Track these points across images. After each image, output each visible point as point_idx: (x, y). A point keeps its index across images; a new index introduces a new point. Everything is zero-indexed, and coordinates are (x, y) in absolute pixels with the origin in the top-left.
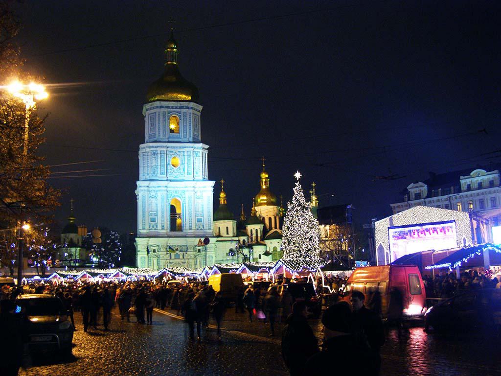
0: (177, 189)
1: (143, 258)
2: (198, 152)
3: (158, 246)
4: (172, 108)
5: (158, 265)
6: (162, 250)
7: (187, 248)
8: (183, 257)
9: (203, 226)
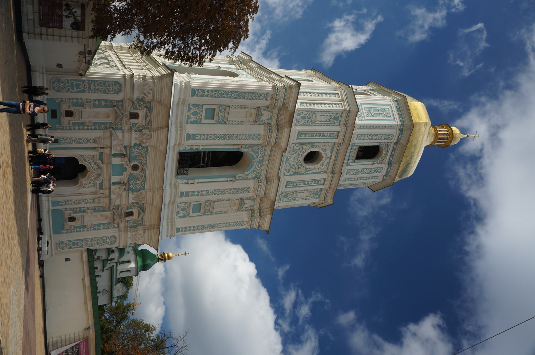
0: (266, 163)
1: (116, 88)
2: (320, 195)
3: (147, 126)
4: (394, 150)
5: (95, 124)
6: (134, 135)
7: (137, 190)
8: (114, 183)
9: (184, 216)
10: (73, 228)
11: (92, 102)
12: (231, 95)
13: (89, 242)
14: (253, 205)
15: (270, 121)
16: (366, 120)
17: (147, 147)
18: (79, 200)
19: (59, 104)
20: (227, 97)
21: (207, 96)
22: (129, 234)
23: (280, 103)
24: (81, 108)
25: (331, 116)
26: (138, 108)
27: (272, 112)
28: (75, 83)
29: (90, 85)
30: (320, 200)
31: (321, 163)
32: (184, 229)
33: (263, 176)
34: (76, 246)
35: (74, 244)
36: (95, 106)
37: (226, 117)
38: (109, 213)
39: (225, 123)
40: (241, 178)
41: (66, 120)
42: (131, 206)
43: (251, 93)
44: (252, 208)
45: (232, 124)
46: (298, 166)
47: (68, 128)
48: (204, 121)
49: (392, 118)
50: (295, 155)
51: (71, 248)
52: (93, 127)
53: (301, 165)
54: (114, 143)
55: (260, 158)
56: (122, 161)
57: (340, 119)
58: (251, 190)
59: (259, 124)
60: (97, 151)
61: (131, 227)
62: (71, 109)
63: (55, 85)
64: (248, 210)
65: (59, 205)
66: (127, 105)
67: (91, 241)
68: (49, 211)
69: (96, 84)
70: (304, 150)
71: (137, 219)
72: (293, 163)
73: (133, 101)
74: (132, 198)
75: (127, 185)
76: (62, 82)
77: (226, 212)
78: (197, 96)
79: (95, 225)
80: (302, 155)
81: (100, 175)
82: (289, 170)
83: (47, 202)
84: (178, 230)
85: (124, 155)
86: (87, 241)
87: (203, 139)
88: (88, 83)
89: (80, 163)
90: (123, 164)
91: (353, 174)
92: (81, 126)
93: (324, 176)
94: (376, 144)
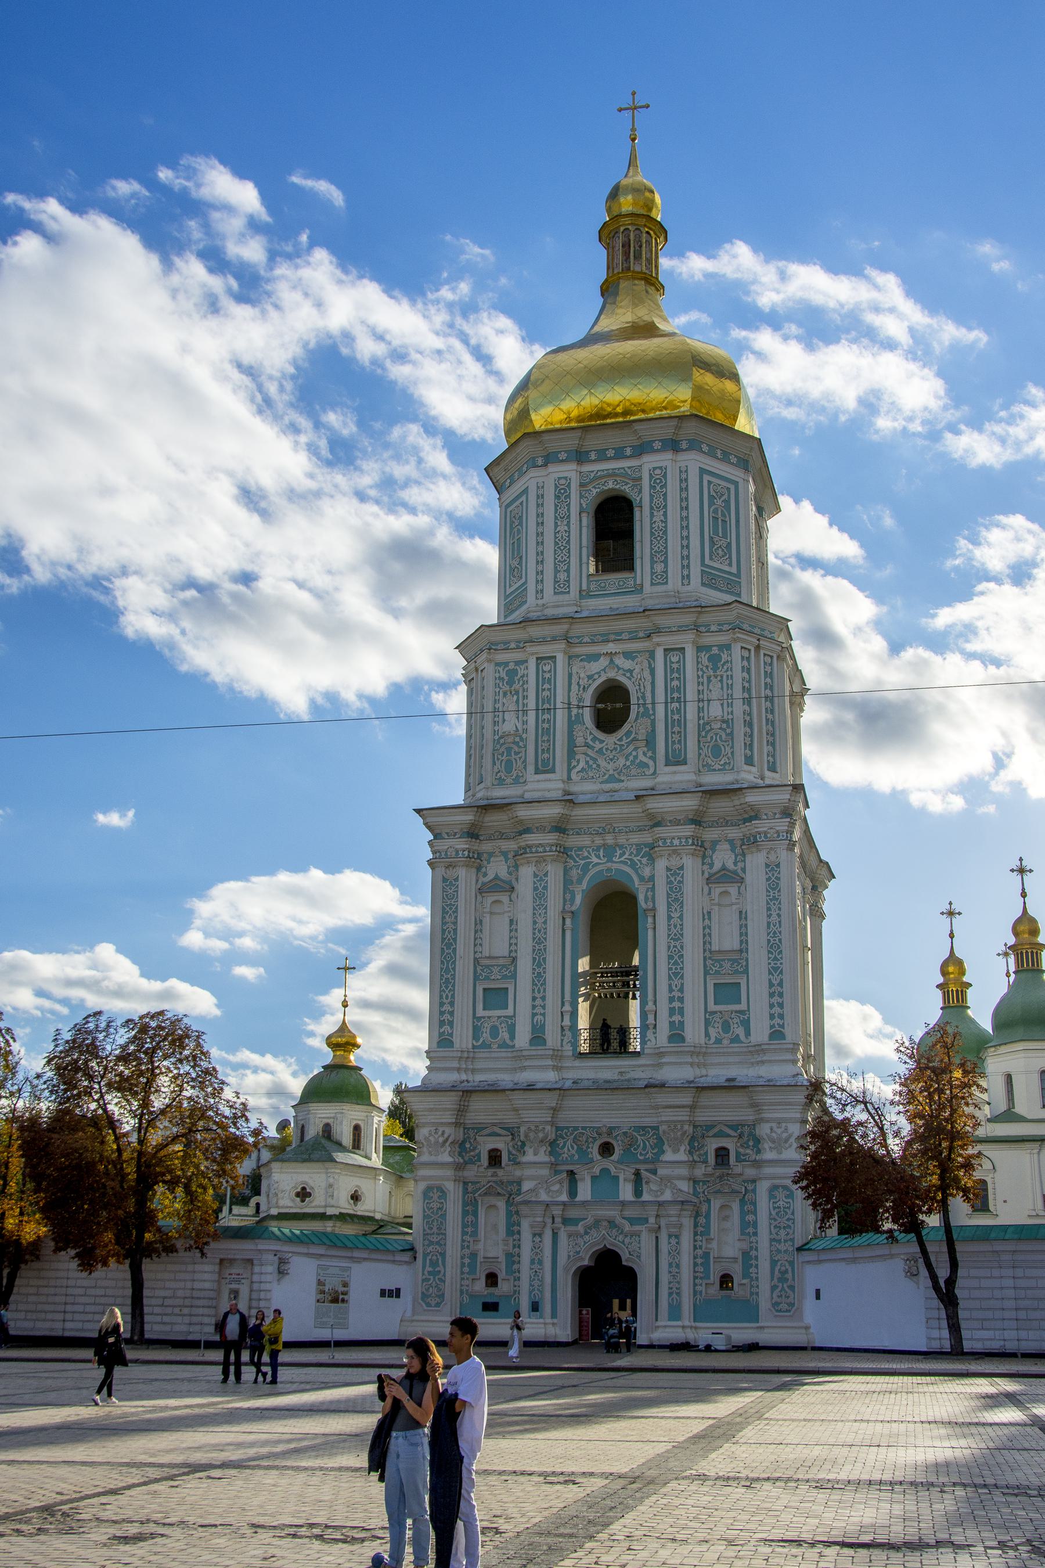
0: (610, 840)
1: (435, 1197)
3: (512, 1132)
5: (510, 1232)
6: (529, 1157)
8: (638, 1193)
9: (746, 1024)
10: (744, 1281)
11: (467, 1238)
12: (448, 962)
13: (782, 1247)
14: (731, 842)
15: (510, 856)
16: (526, 582)
17: (558, 1129)
18: (670, 1265)
19: (471, 1296)
20: (454, 969)
21: (452, 1013)
22: (769, 1155)
24: (480, 1259)
25: (505, 694)
26: (477, 1151)
27: (491, 854)
28: (428, 1269)
29: (431, 1243)
30: (735, 640)
31: (623, 680)
32: (777, 1021)
34: (789, 1276)
35: (782, 1279)
36: (475, 1233)
37: (501, 962)
39: (514, 960)
40: (650, 894)
41: (504, 1287)
42: (699, 1156)
43: (443, 918)
44: (739, 843)
45: (516, 944)
46: (629, 744)
47: (516, 1283)
48: (510, 1011)
49: (524, 498)
50: (602, 762)
51: (792, 1288)
52: (516, 1237)
53: (628, 733)
54: (544, 1197)
55: (598, 857)
56: (583, 1179)
57: (511, 666)
58: (675, 862)
59: (517, 879)
60: (559, 1229)
61: (759, 1151)
63: (433, 1303)
64: (744, 855)
65: (679, 1305)
66: (470, 1173)
67: (779, 1241)
68: (696, 1328)
69: (429, 1231)
70: (589, 741)
71: (736, 1140)
72: (622, 761)
73: (466, 1163)
74: (675, 1155)
75: (638, 1166)
76: (427, 1290)
77: (742, 915)
78: (451, 1035)
79: (743, 1233)
80: (602, 742)
81: (612, 1224)
83: (667, 1330)
84: (777, 1034)
85: (571, 1173)
86: (779, 1251)
87: (544, 1007)
88: (429, 1245)
89: (586, 1263)
90: (594, 1178)
91: (665, 562)
92: (512, 1259)
94: (588, 521)
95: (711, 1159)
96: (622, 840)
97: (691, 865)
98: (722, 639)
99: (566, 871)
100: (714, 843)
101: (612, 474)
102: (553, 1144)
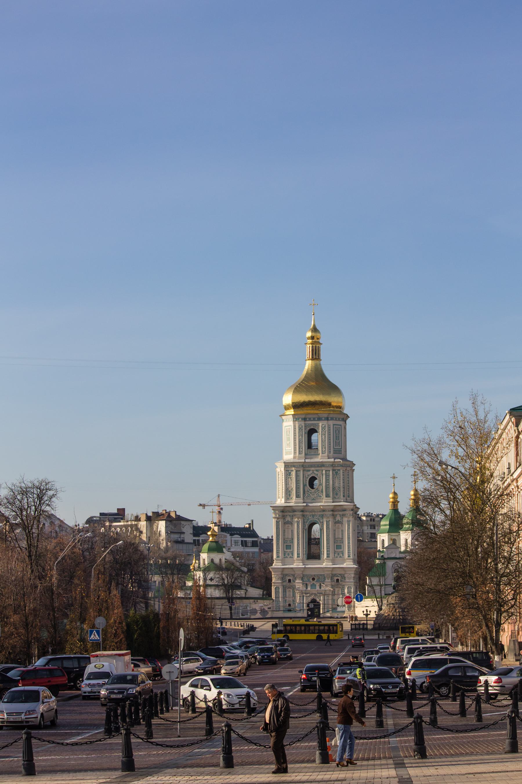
0: (313, 513)
3: (293, 575)
4: (310, 420)
8: (320, 588)
9: (343, 554)
23: (281, 514)
33: (322, 513)
38: (336, 590)
41: (292, 607)
58: (328, 520)
62: (287, 604)
66: (284, 584)
82: (320, 496)
84: (349, 556)
92: (294, 601)
93: (324, 472)
95: (335, 581)
96: (316, 513)
97: (331, 519)
98: (338, 468)
99: (304, 520)
100: (336, 515)
101: (313, 424)
102: (302, 578)
